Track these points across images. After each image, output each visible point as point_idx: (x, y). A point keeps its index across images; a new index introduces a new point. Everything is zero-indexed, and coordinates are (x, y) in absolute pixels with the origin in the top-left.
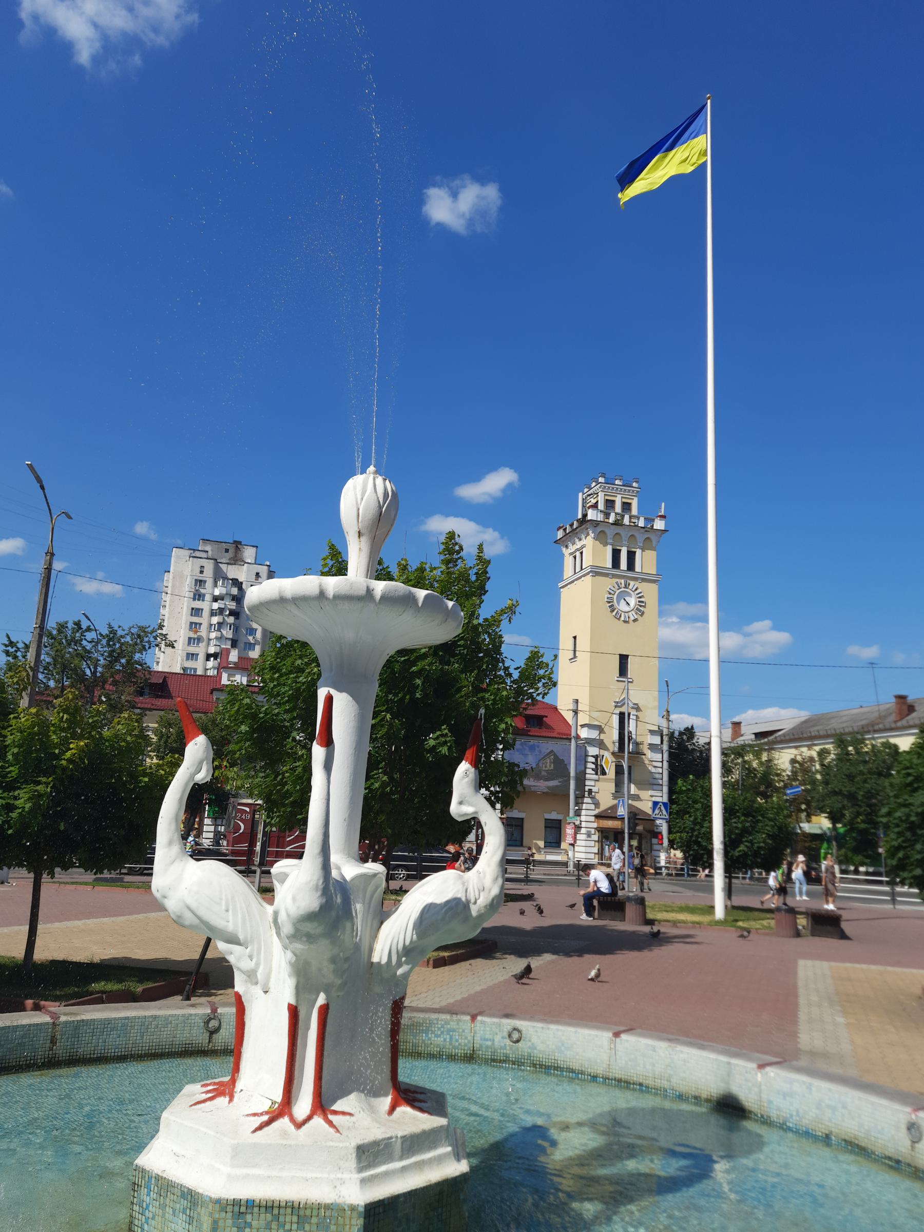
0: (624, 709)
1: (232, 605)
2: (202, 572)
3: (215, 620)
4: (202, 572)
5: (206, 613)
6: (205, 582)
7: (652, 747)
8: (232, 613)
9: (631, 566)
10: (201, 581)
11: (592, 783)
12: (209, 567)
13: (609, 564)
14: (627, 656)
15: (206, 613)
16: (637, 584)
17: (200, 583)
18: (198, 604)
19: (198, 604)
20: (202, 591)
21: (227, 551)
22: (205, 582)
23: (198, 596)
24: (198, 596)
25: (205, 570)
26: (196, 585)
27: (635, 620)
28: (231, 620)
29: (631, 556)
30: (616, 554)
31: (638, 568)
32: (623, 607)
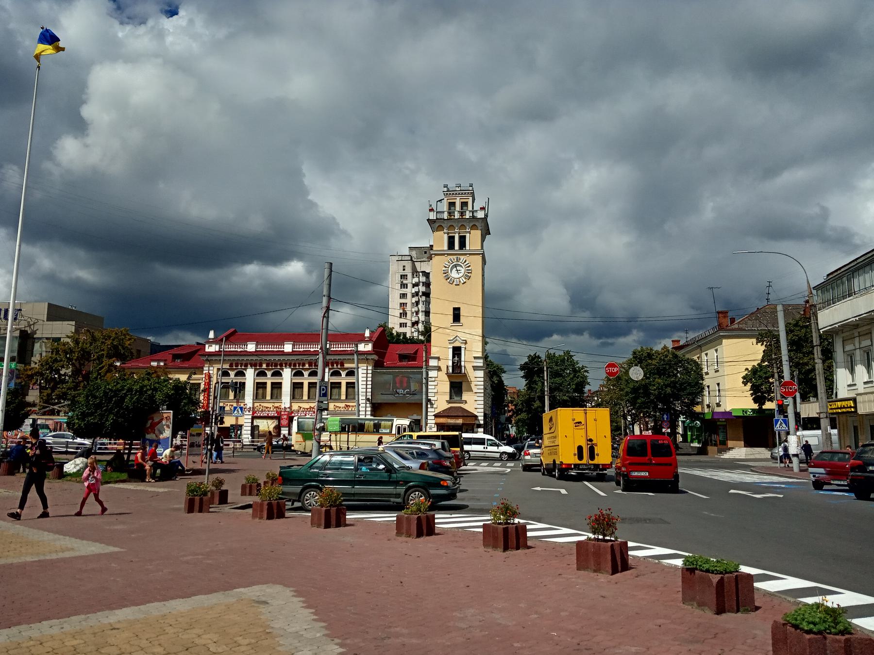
0: (457, 344)
1: (422, 289)
3: (414, 300)
5: (409, 296)
7: (475, 368)
8: (424, 294)
9: (462, 245)
11: (433, 395)
12: (408, 265)
13: (446, 248)
14: (458, 309)
15: (409, 296)
17: (403, 277)
18: (404, 291)
19: (404, 291)
20: (405, 282)
23: (404, 286)
24: (404, 286)
28: (424, 298)
29: (463, 240)
30: (451, 240)
31: (467, 248)
32: (454, 274)
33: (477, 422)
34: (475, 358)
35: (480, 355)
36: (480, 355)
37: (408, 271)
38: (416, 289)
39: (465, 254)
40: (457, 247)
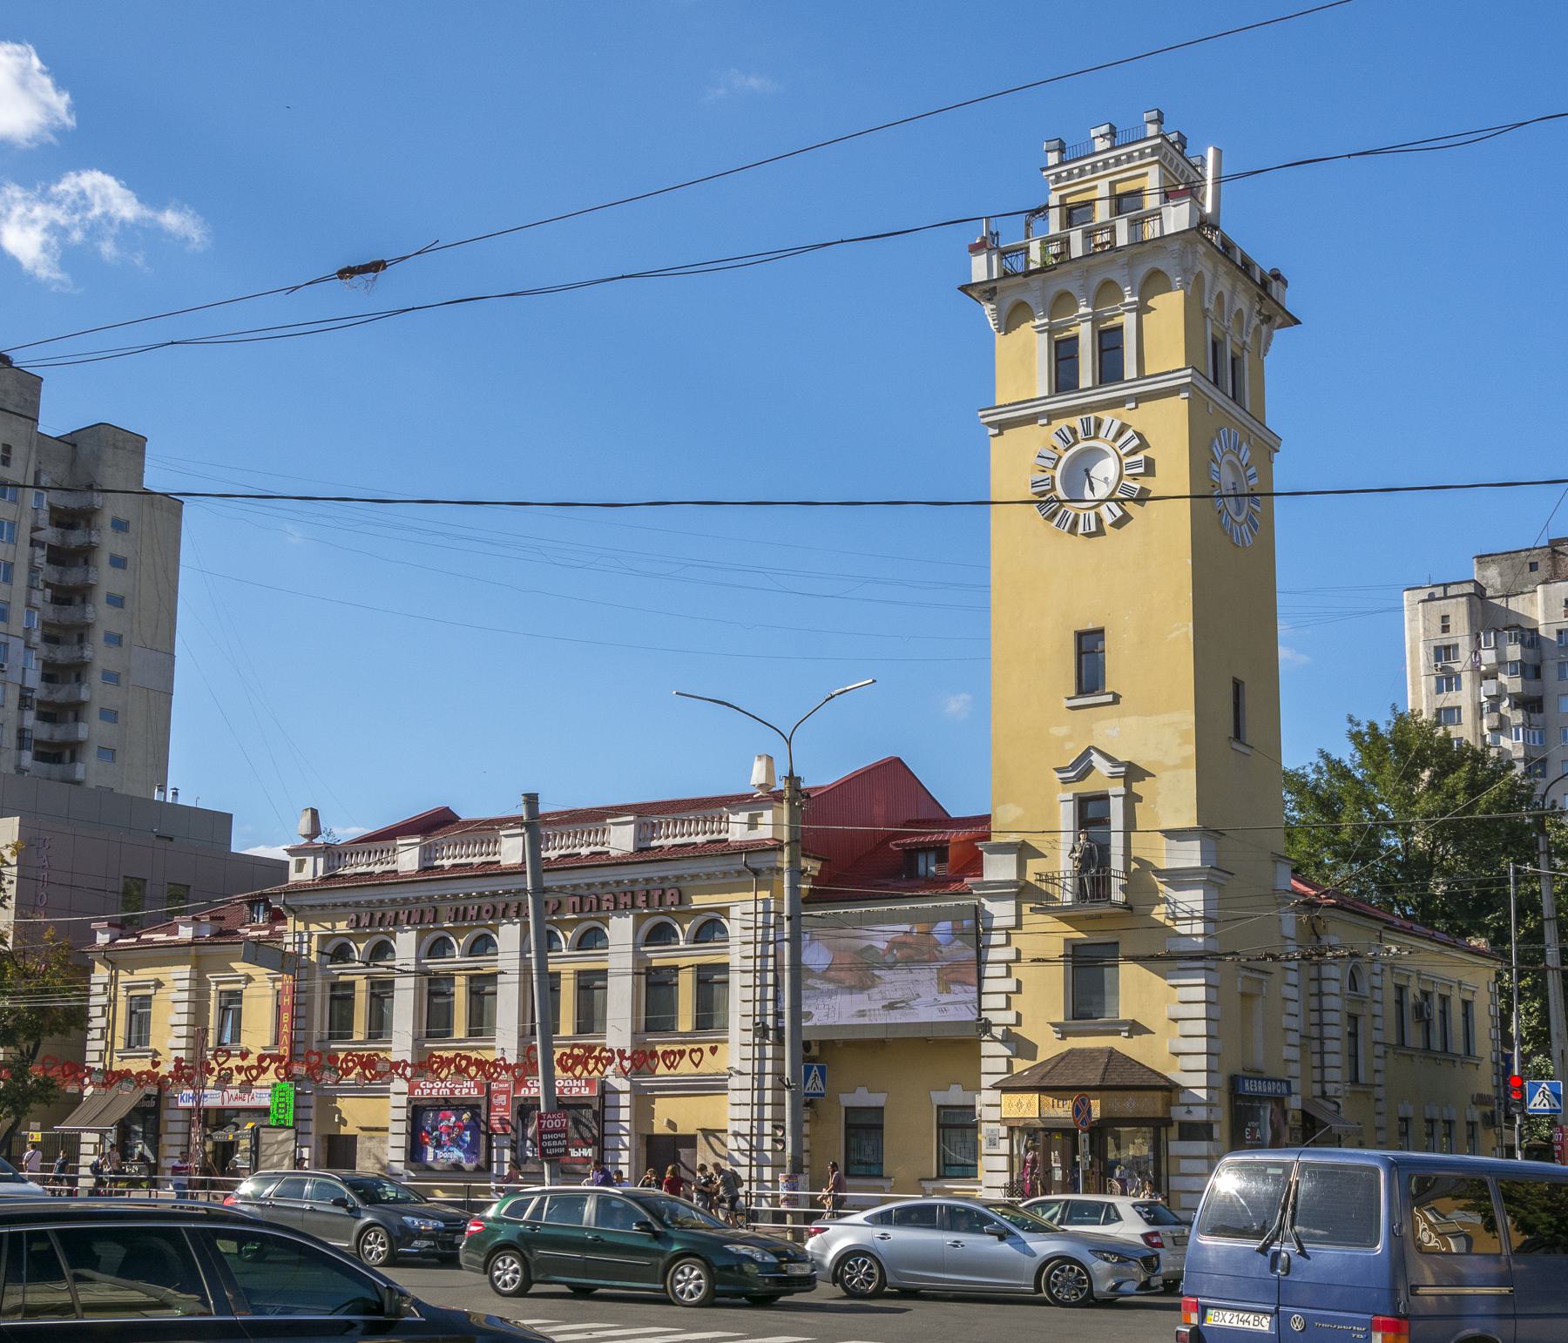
2: (1445, 629)
4: (1445, 629)
5: (1467, 715)
6: (1456, 646)
9: (1109, 371)
10: (1447, 648)
15: (1467, 715)
16: (1124, 414)
17: (1444, 653)
21: (1533, 567)
22: (1456, 646)
25: (1452, 622)
26: (1438, 658)
27: (1119, 524)
29: (1109, 342)
30: (1064, 355)
33: (1179, 1114)
34: (1170, 834)
35: (1189, 820)
36: (1189, 820)
37: (1460, 633)
38: (1490, 687)
39: (1118, 403)
40: (1086, 378)
